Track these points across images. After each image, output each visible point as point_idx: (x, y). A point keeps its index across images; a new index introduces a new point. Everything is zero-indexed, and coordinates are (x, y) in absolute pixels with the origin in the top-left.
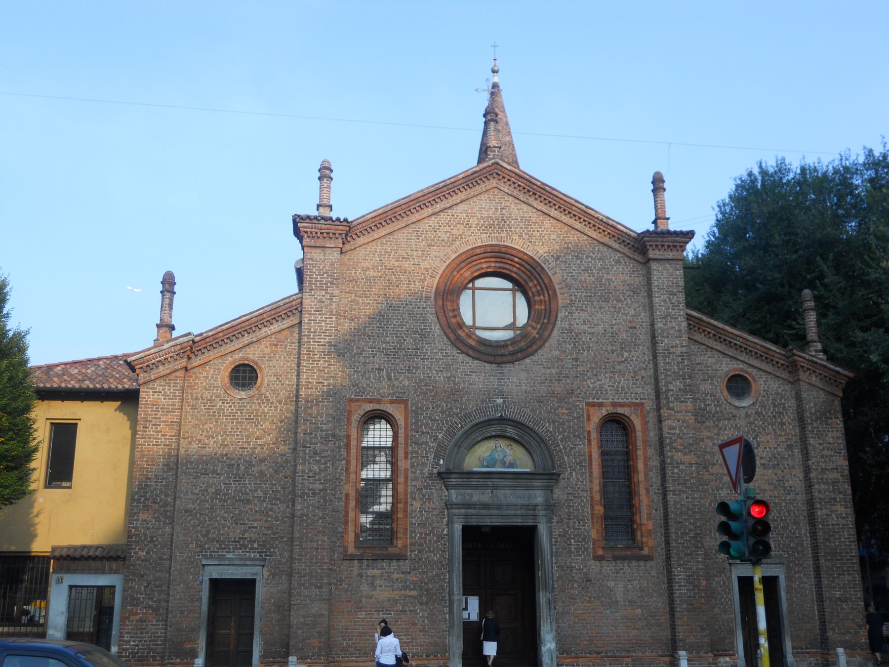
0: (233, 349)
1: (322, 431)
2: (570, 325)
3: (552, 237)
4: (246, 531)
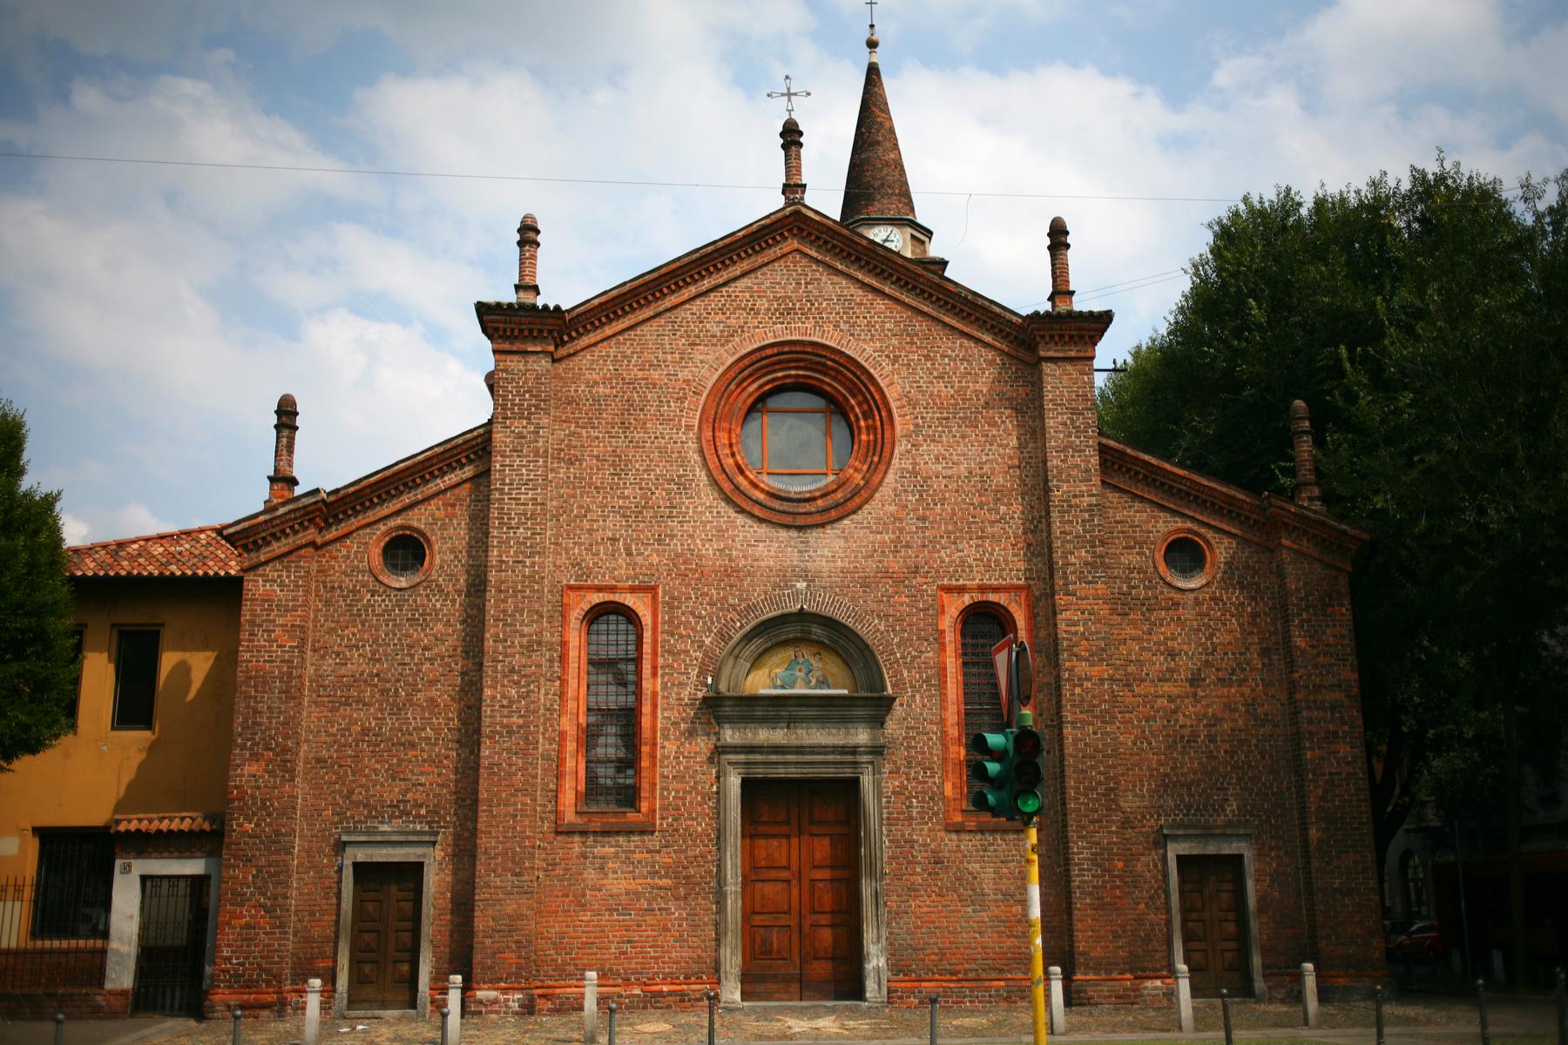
1: (523, 636)
4: (408, 790)
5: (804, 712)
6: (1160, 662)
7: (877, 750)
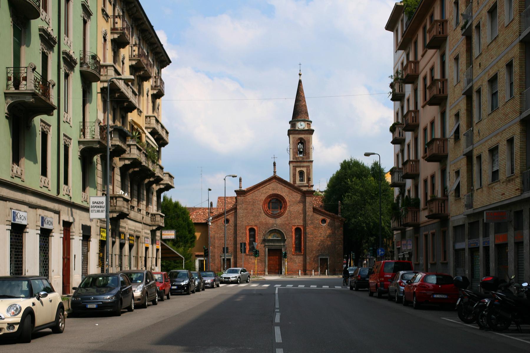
7: (284, 246)
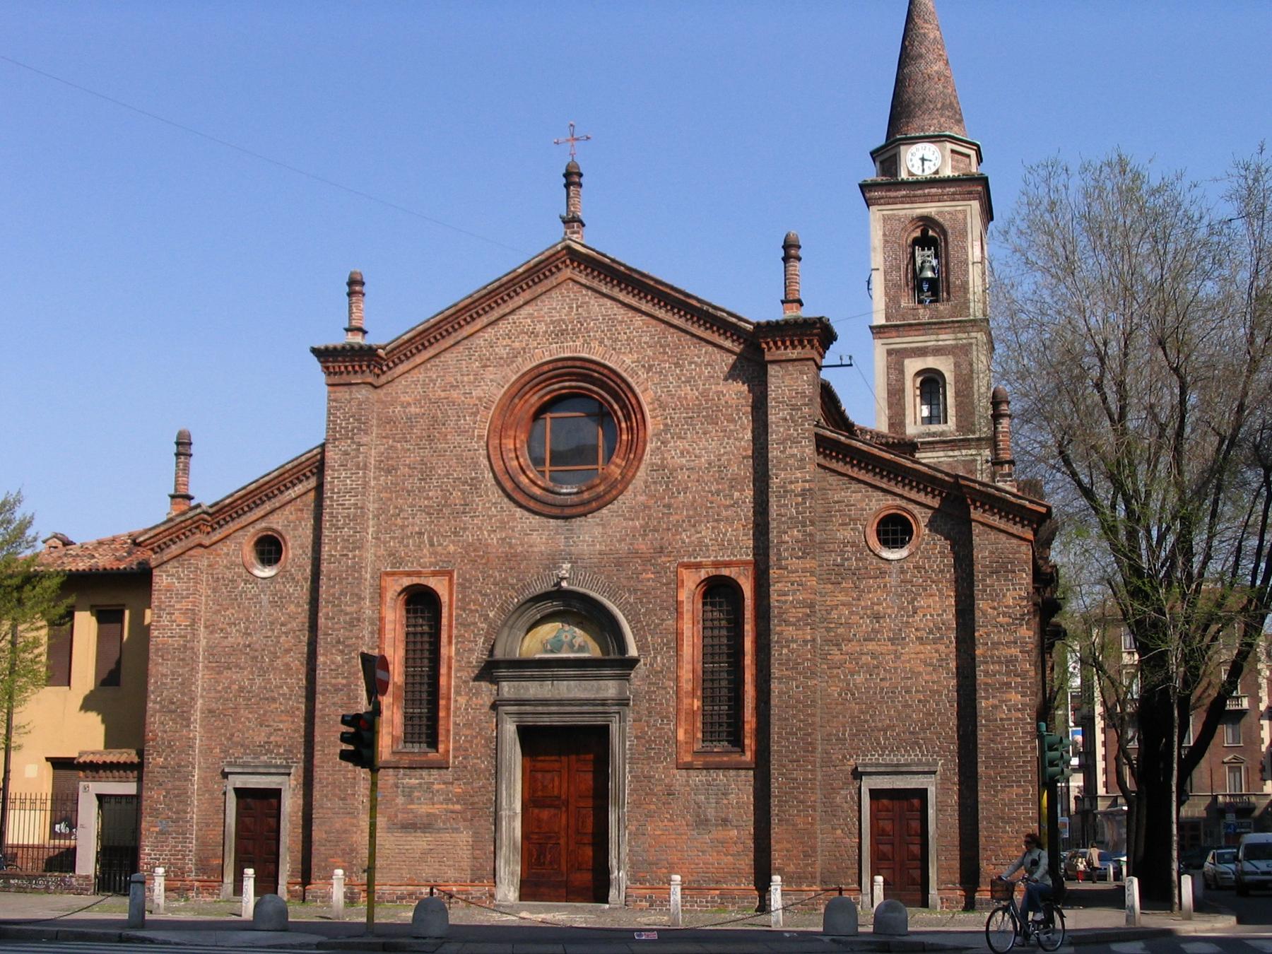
0: (255, 517)
1: (346, 614)
2: (663, 459)
3: (644, 339)
4: (271, 734)
5: (563, 672)
6: (866, 625)
7: (623, 702)
